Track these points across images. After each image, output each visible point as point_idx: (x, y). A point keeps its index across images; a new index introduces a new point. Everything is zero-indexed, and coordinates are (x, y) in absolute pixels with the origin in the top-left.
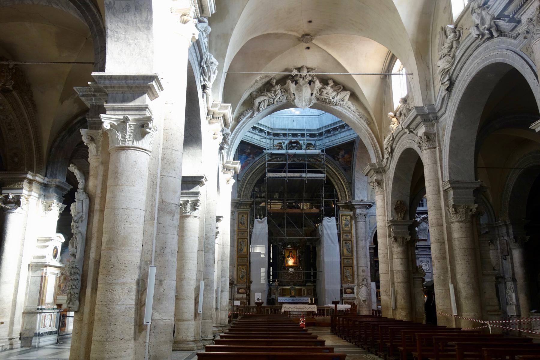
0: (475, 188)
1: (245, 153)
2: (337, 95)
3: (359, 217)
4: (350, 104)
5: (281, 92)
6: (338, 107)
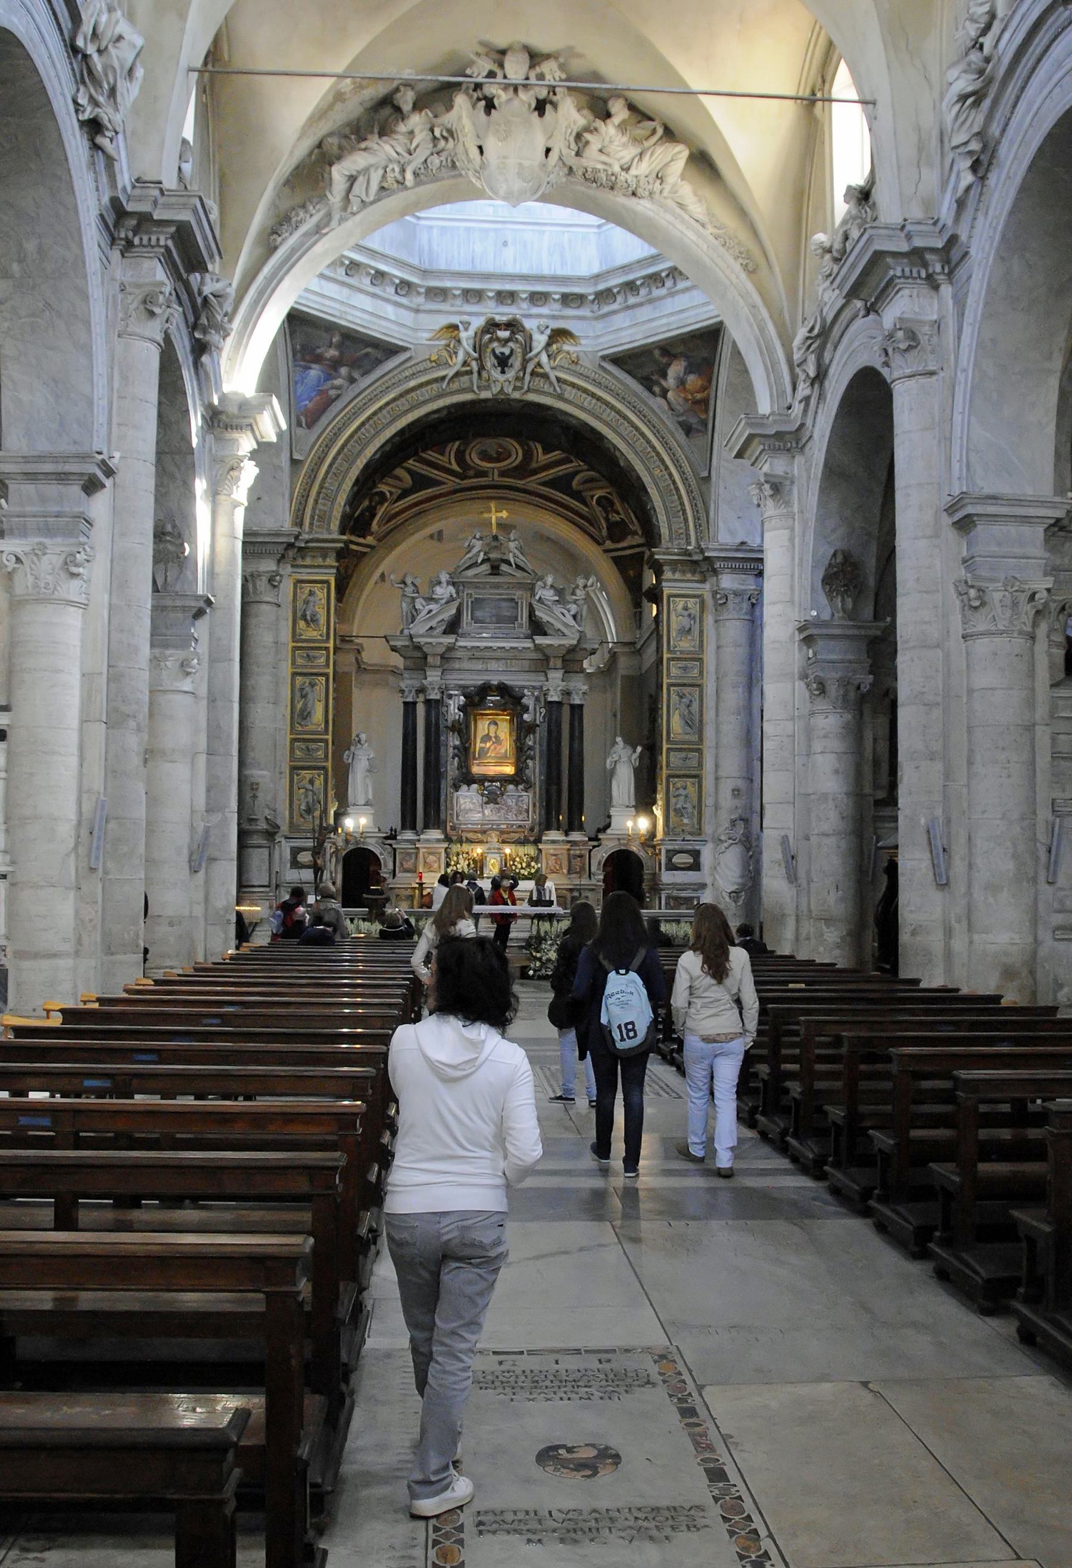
0: (1052, 521)
1: (318, 359)
2: (641, 159)
3: (730, 603)
4: (686, 191)
6: (642, 201)
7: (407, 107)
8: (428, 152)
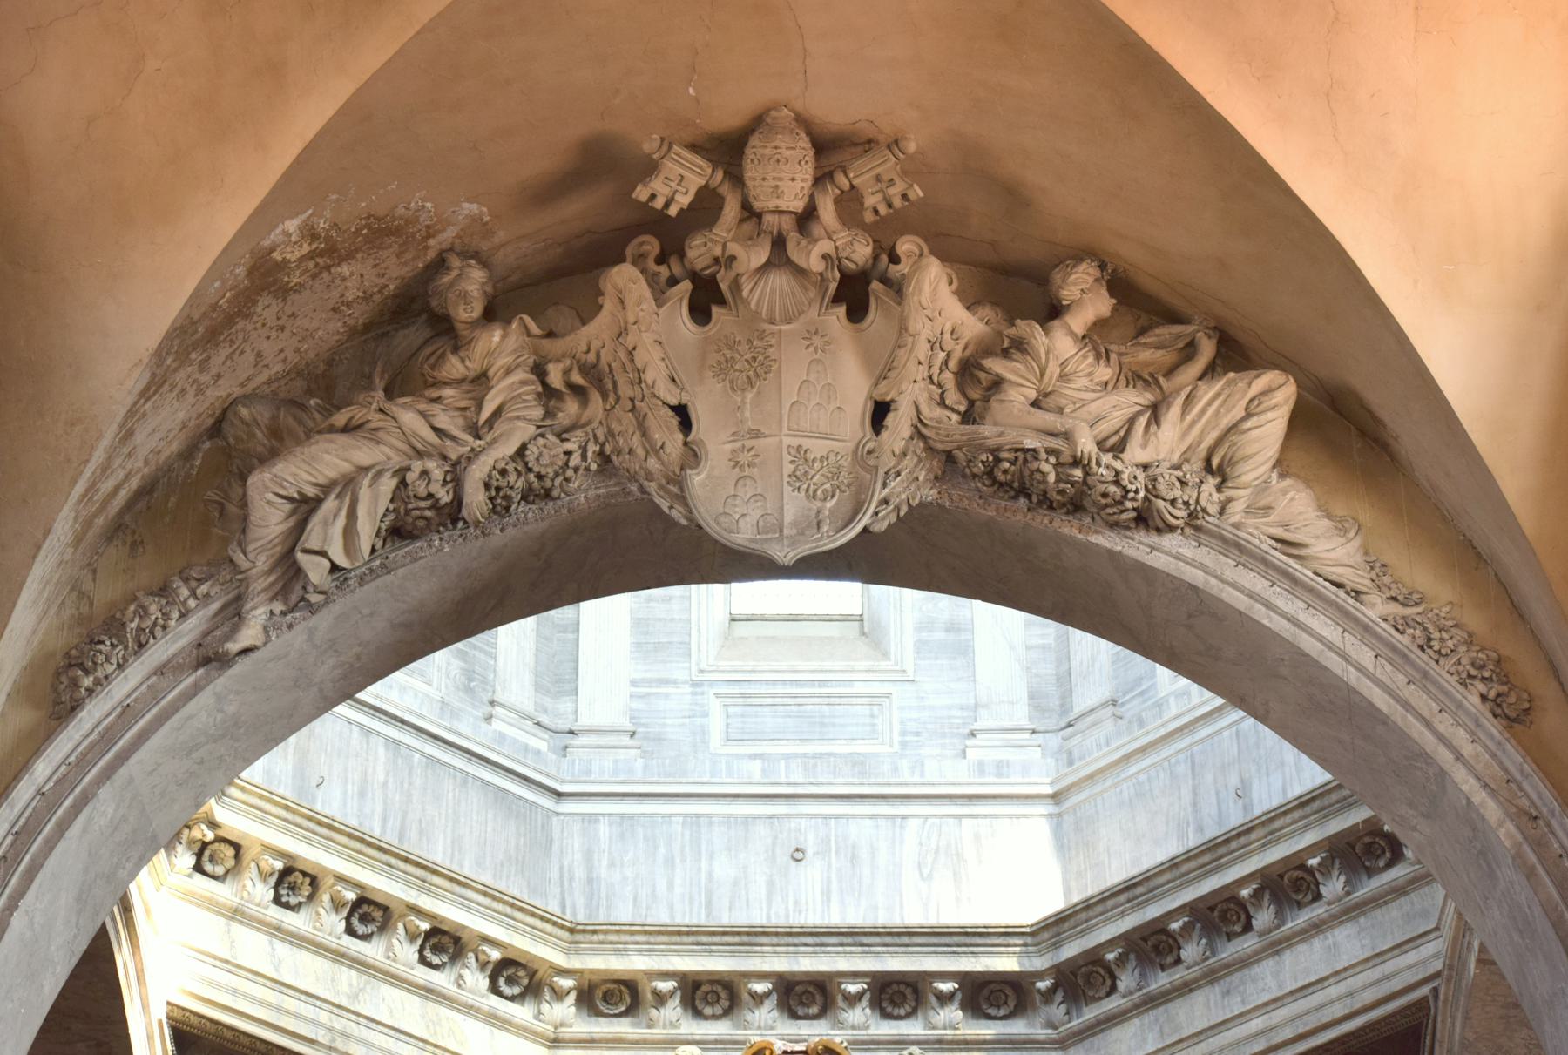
5: (548, 394)
6: (1169, 541)
7: (467, 313)
8: (532, 430)
